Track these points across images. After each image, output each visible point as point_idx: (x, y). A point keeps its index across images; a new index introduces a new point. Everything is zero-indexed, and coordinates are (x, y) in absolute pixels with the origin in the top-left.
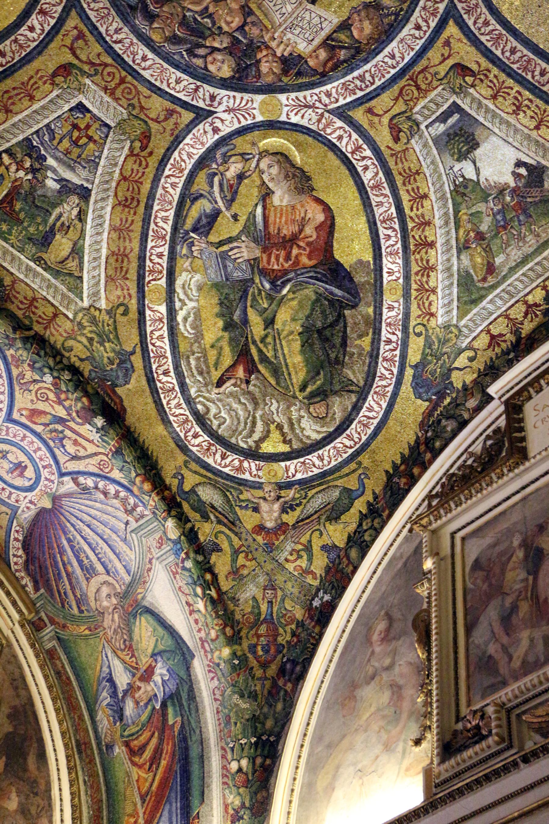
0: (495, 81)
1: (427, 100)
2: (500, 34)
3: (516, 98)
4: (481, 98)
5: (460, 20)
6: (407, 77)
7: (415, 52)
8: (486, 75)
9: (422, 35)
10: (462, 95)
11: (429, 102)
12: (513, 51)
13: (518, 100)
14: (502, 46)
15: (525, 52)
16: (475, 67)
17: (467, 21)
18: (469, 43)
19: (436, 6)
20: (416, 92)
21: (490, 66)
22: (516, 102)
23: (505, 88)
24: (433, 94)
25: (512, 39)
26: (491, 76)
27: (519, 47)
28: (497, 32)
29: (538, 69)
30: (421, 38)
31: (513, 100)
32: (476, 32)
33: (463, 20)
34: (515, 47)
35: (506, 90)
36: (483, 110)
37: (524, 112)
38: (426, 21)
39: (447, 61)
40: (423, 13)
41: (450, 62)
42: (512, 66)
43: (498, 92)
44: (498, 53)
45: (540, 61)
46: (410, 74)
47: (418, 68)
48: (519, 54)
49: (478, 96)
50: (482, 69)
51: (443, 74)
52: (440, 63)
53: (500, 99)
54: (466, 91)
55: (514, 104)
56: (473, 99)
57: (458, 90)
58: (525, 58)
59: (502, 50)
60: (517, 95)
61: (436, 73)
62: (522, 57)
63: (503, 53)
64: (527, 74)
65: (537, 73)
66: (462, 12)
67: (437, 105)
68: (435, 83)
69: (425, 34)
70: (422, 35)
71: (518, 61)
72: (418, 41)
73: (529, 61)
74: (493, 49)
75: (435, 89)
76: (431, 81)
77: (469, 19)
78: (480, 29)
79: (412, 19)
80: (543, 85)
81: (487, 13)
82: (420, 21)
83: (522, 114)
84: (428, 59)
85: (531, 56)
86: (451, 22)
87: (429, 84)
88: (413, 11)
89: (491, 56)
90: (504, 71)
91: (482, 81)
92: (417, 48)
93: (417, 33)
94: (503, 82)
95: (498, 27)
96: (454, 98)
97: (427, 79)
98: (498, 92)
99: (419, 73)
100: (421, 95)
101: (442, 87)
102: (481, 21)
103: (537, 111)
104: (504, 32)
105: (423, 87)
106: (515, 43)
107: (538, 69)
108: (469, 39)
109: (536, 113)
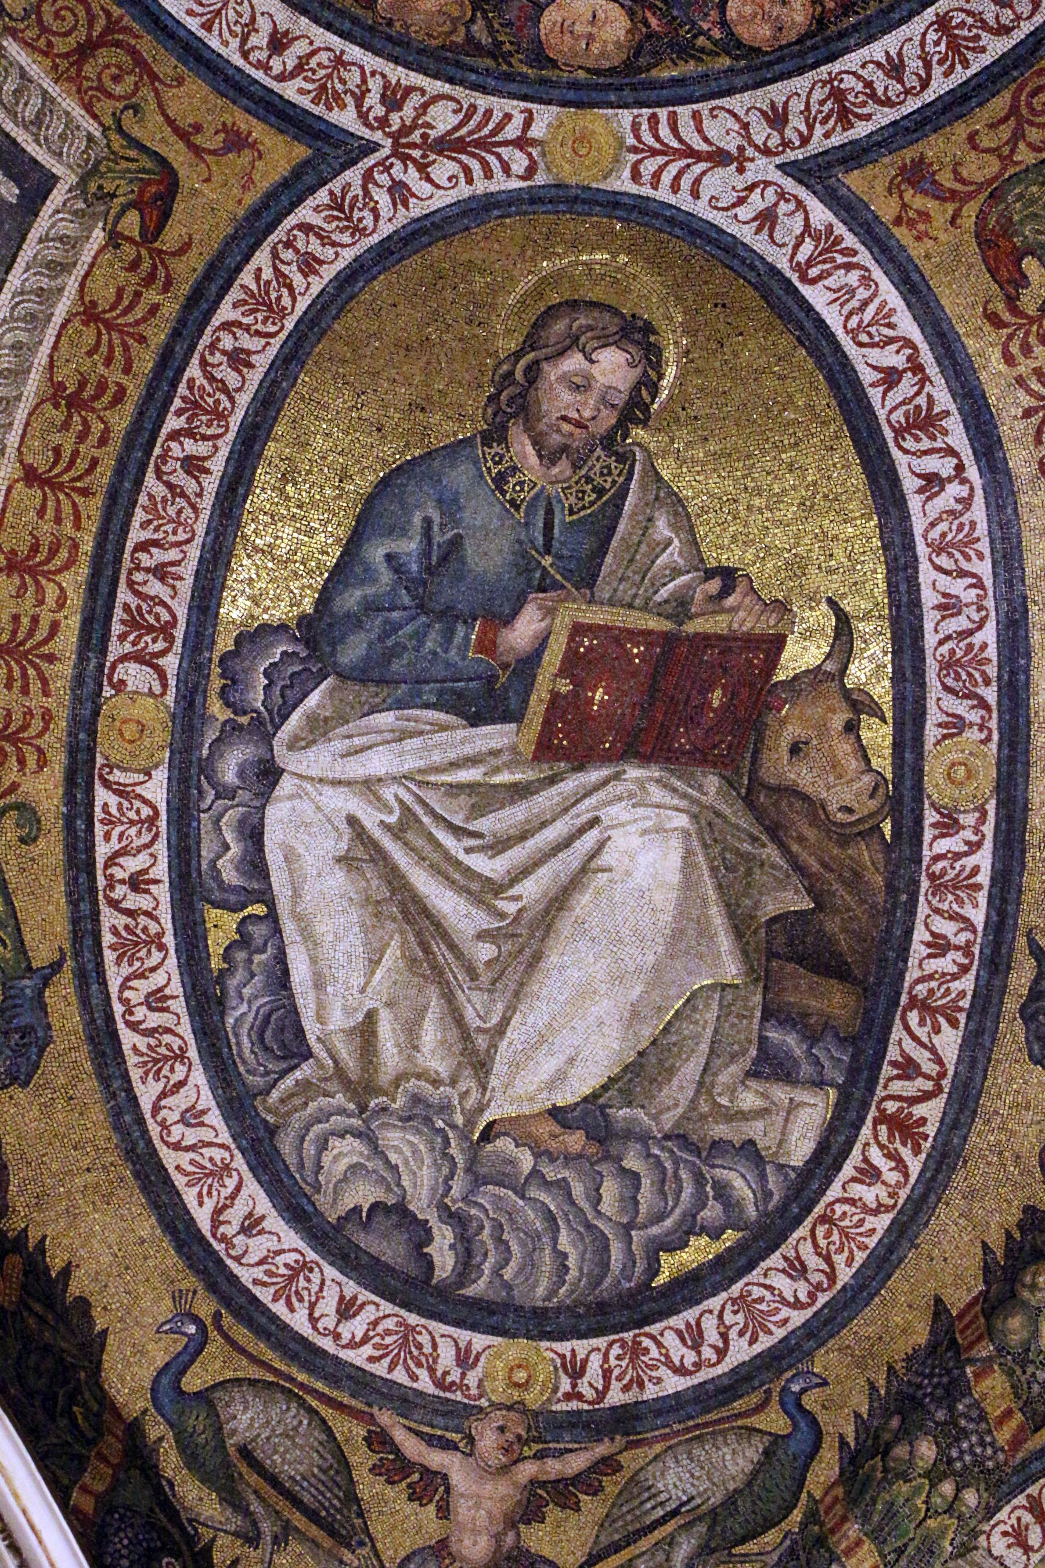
0: (138, 313)
1: (47, 84)
2: (282, 312)
3: (102, 387)
4: (80, 270)
5: (309, 179)
6: (117, 11)
7: (201, 33)
8: (150, 279)
9: (254, 56)
10: (81, 205)
11: (45, 93)
12: (239, 359)
13: (96, 397)
14: (245, 320)
15: (244, 399)
16: (172, 236)
17: (310, 202)
18: (241, 213)
19: (349, 99)
20: (72, 41)
21: (185, 289)
22: (89, 392)
23: (126, 348)
24: (70, 104)
25: (272, 351)
26: (152, 296)
27: (255, 377)
28: (286, 301)
29: (202, 449)
30: (245, 55)
31: (93, 379)
32: (278, 234)
33: (312, 190)
34: (250, 366)
35: (118, 351)
36: (45, 283)
37: (66, 426)
38: (300, 68)
39: (181, 145)
40: (324, 57)
41: (177, 154)
42: (195, 361)
43: (109, 326)
44: (226, 312)
45: (224, 452)
46: (127, 21)
47: (147, 45)
48: (232, 379)
49: (86, 258)
50: (173, 263)
51: (136, 132)
52: (170, 122)
53: (89, 336)
54: (94, 216)
55: (82, 385)
56: (71, 243)
57: (93, 187)
58: (226, 403)
59: (239, 325)
60: (113, 389)
61: (136, 109)
62: (225, 391)
63: (227, 326)
64: (179, 413)
65: (191, 447)
66: (336, 185)
67: (38, 121)
68: (106, 107)
69: (259, 65)
70: (254, 56)
71: (211, 379)
72: (235, 43)
73: (221, 416)
74: (235, 294)
75: (88, 108)
76: (110, 96)
77: (317, 209)
78: (289, 244)
79: (304, 21)
80: (159, 474)
81: (341, 264)
82: (300, 48)
83: (59, 416)
84: (180, 81)
85: (235, 421)
86: (301, 152)
87: (101, 88)
88: (329, 27)
89: (214, 288)
90: (176, 334)
91: (134, 266)
92: (214, 43)
93: (260, 39)
94: (142, 339)
95: (302, 304)
96: (67, 178)
97: (116, 79)
98: (109, 326)
99: (133, 52)
100: (63, 64)
101: (97, 134)
102: (315, 246)
103: (82, 465)
104: (290, 324)
105: (89, 70)
106: (262, 362)
107: (202, 449)
108: (256, 213)
109: (72, 463)
